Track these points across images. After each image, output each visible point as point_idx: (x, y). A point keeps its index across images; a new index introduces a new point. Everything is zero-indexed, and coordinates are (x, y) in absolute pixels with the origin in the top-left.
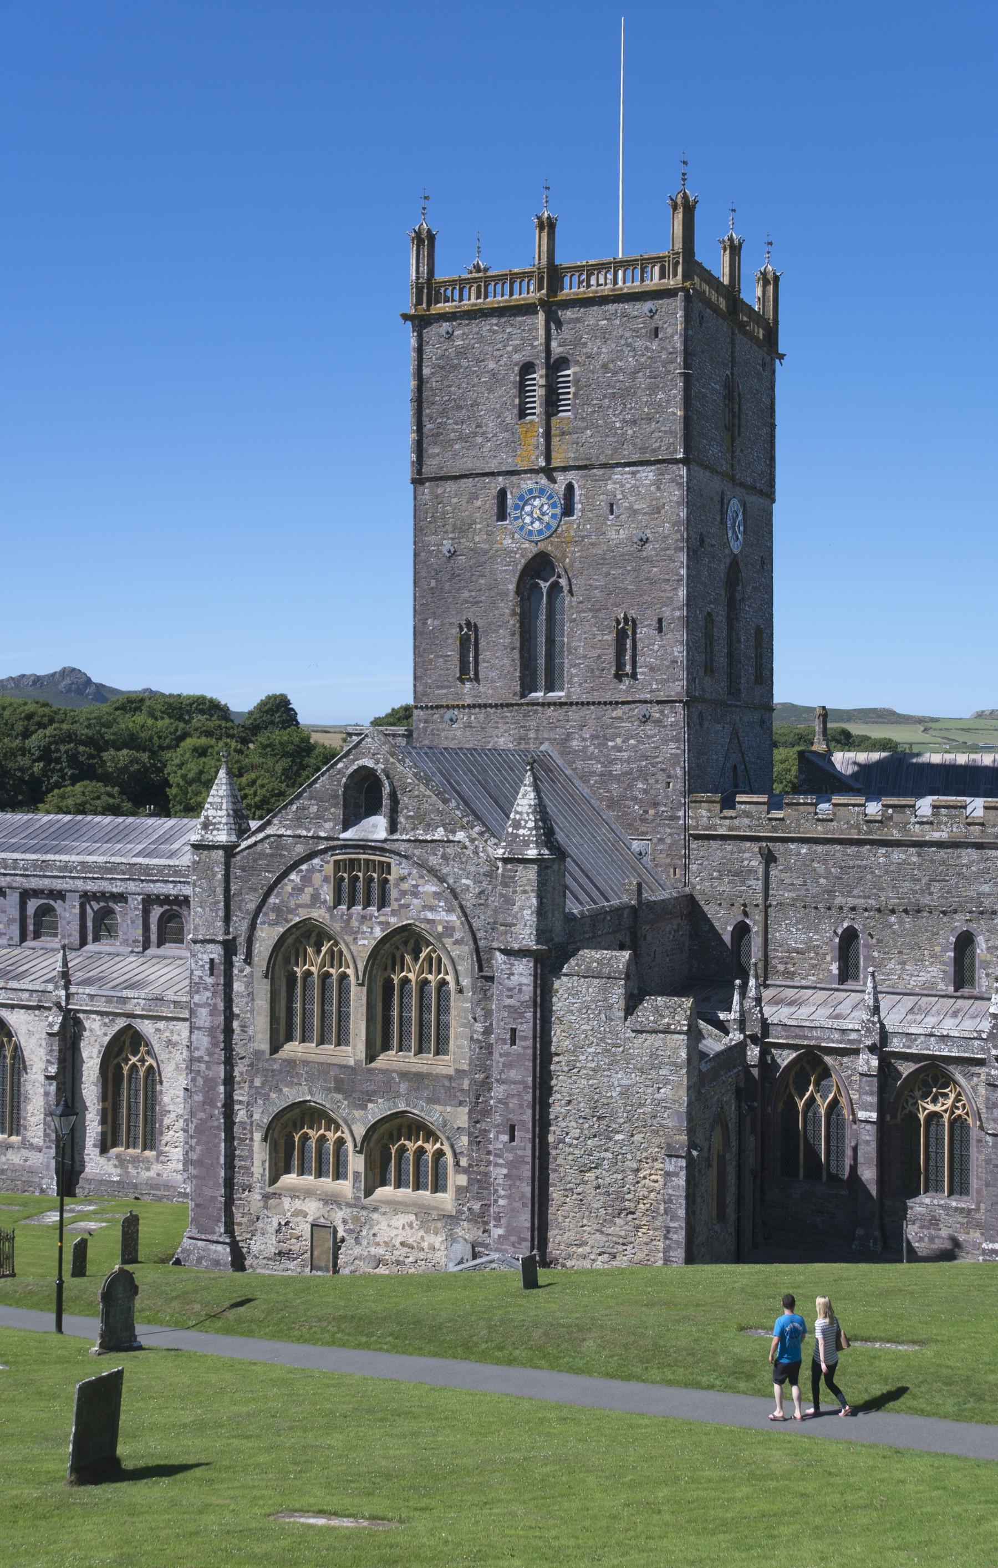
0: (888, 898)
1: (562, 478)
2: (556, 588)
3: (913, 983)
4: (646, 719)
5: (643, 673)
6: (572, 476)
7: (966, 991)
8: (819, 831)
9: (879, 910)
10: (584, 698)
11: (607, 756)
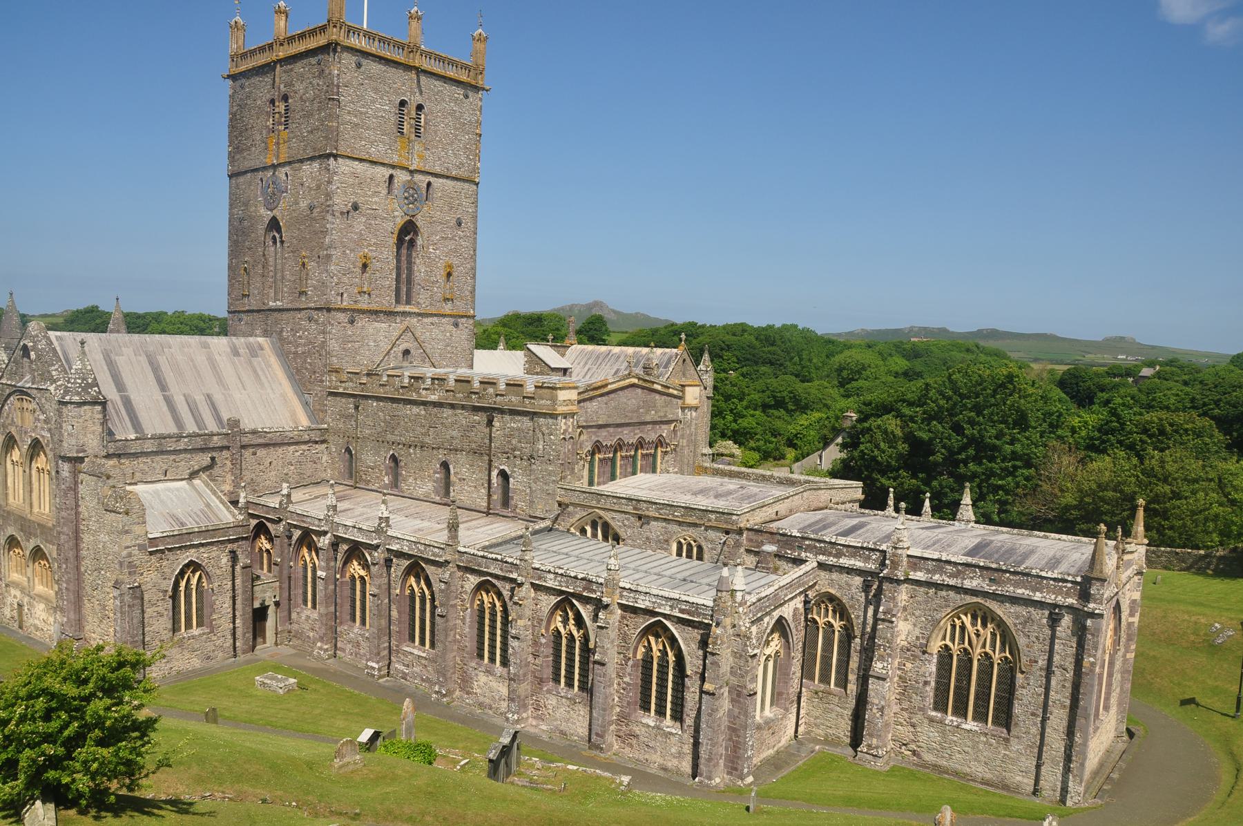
0: (410, 437)
2: (281, 237)
3: (420, 492)
4: (310, 319)
5: (311, 291)
6: (287, 169)
8: (381, 392)
9: (404, 445)
10: (289, 306)
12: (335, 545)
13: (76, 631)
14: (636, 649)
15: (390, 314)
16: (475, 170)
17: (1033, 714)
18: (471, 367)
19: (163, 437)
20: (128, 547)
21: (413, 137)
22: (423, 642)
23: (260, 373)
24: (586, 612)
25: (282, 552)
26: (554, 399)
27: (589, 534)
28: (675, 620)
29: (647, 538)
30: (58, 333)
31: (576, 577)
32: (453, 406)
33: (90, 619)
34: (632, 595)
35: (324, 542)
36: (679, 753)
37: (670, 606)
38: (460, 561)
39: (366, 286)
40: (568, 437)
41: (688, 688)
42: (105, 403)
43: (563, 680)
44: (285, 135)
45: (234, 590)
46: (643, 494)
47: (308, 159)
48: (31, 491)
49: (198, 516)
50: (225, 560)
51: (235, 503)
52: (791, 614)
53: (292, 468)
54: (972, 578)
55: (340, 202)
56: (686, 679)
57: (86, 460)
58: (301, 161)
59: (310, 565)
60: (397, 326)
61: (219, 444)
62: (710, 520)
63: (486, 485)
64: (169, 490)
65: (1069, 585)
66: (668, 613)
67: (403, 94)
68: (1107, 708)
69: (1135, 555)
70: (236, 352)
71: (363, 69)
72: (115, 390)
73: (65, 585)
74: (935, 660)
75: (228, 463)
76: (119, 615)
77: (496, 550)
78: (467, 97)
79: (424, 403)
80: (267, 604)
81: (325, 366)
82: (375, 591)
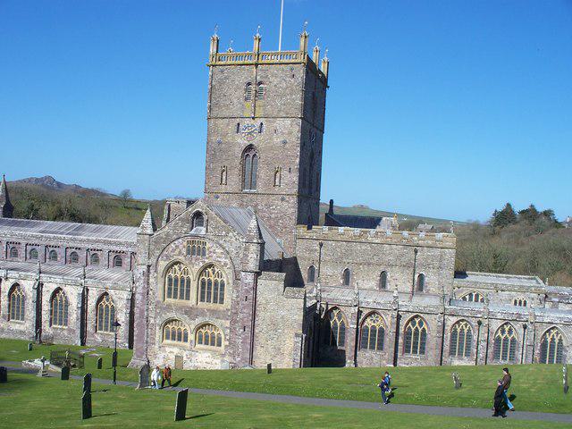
1: (258, 121)
4: (283, 200)
6: (263, 120)
8: (339, 238)
12: (360, 312)
24: (518, 327)
44: (259, 103)
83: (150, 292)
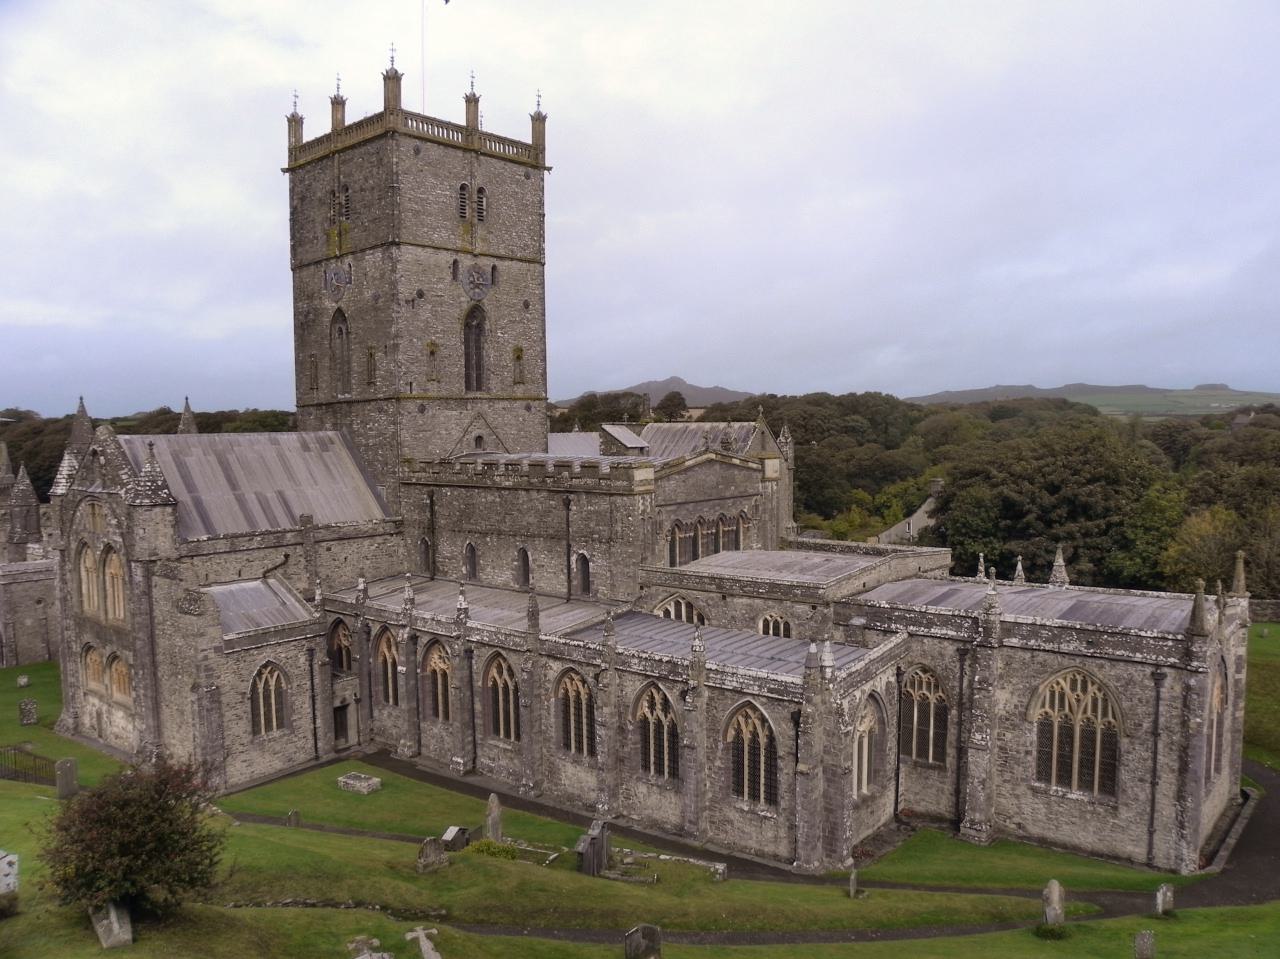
3: (500, 580)
4: (380, 410)
7: (525, 588)
11: (366, 433)
12: (414, 639)
13: (155, 738)
14: (726, 731)
15: (462, 401)
16: (541, 251)
17: (1141, 780)
18: (546, 450)
19: (236, 536)
20: (203, 650)
21: (476, 221)
22: (508, 735)
23: (332, 467)
25: (362, 648)
26: (630, 479)
27: (673, 616)
28: (764, 700)
29: (733, 617)
30: (127, 437)
31: (660, 660)
32: (527, 490)
33: (168, 724)
34: (719, 676)
35: (404, 634)
36: (776, 837)
37: (759, 686)
38: (541, 649)
39: (434, 374)
40: (646, 517)
41: (781, 770)
42: (176, 505)
43: (652, 768)
45: (313, 689)
46: (726, 573)
47: (371, 248)
48: (105, 597)
49: (274, 615)
50: (303, 659)
51: (311, 599)
52: (884, 688)
53: (368, 562)
54: (1069, 642)
55: (405, 291)
56: (779, 761)
57: (159, 563)
58: (363, 251)
59: (390, 661)
60: (469, 412)
61: (293, 541)
62: (796, 595)
63: (566, 571)
64: (244, 590)
65: (1170, 643)
66: (757, 693)
67: (465, 179)
68: (1218, 770)
69: (1239, 609)
70: (305, 447)
71: (421, 155)
72: (186, 491)
73: (142, 691)
74: (1035, 729)
75: (302, 559)
76: (197, 720)
77: (579, 637)
78: (527, 177)
79: (498, 489)
80: (347, 702)
81: (398, 456)
82: (458, 684)
83: (69, 597)
